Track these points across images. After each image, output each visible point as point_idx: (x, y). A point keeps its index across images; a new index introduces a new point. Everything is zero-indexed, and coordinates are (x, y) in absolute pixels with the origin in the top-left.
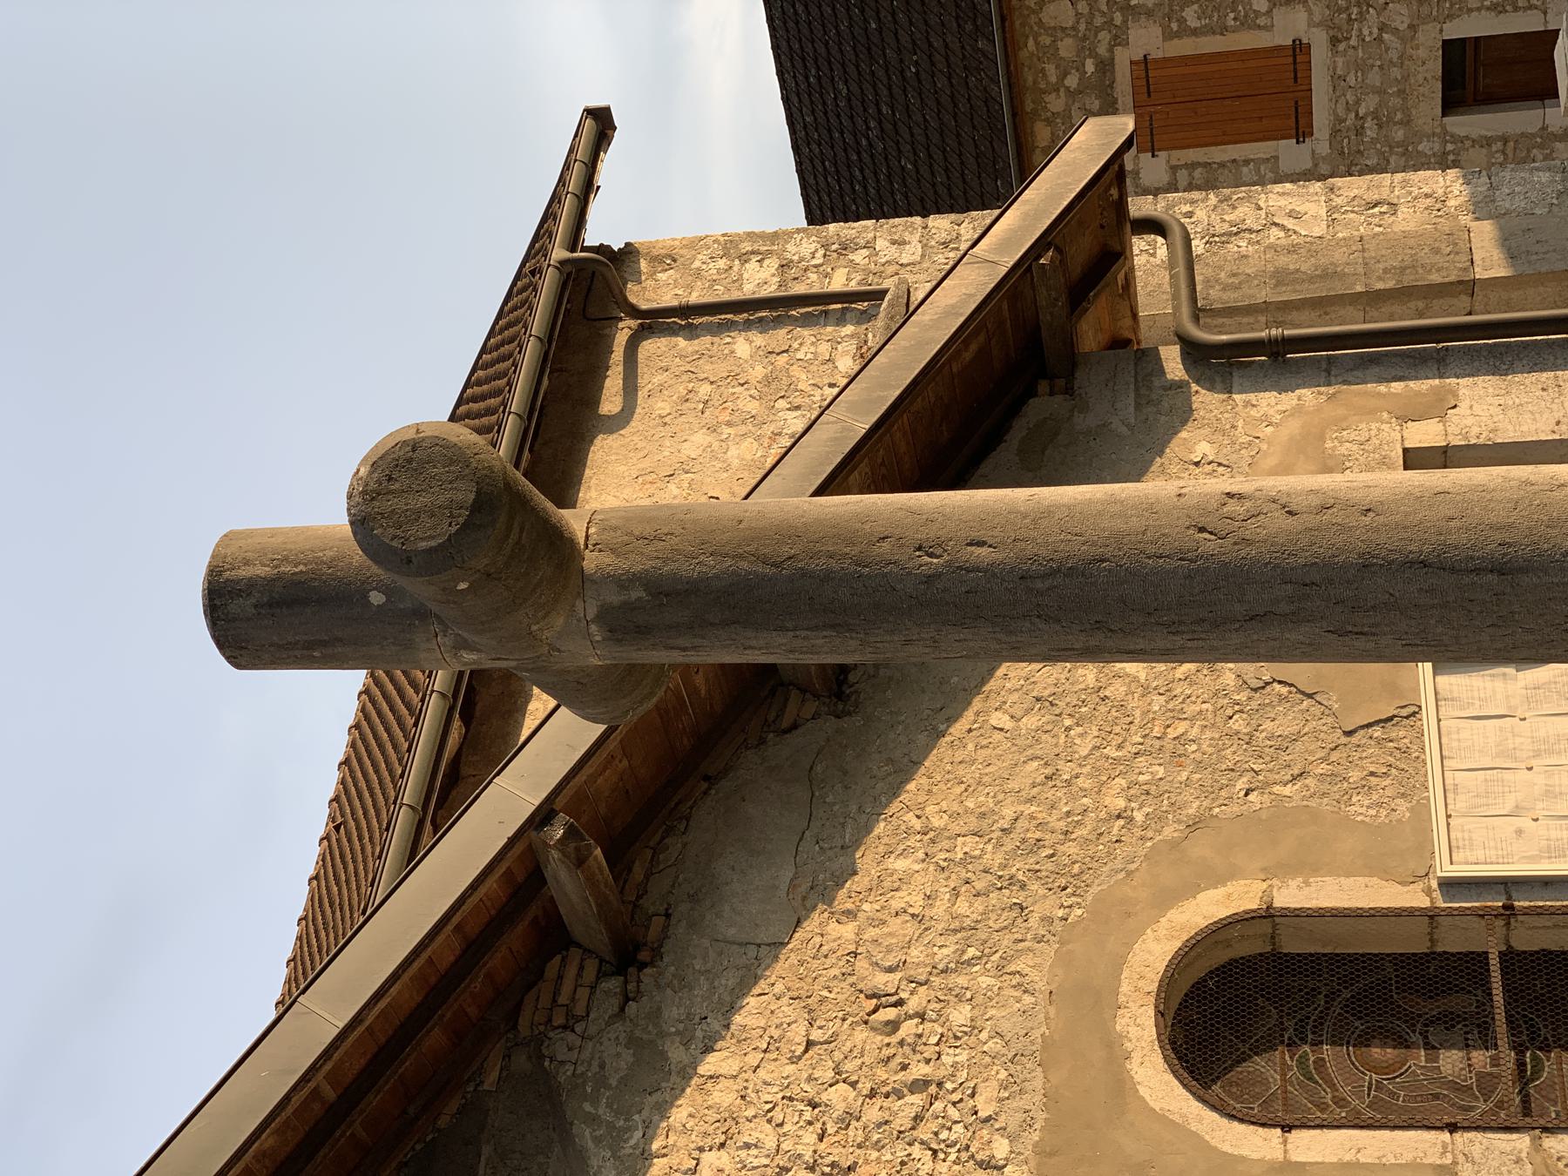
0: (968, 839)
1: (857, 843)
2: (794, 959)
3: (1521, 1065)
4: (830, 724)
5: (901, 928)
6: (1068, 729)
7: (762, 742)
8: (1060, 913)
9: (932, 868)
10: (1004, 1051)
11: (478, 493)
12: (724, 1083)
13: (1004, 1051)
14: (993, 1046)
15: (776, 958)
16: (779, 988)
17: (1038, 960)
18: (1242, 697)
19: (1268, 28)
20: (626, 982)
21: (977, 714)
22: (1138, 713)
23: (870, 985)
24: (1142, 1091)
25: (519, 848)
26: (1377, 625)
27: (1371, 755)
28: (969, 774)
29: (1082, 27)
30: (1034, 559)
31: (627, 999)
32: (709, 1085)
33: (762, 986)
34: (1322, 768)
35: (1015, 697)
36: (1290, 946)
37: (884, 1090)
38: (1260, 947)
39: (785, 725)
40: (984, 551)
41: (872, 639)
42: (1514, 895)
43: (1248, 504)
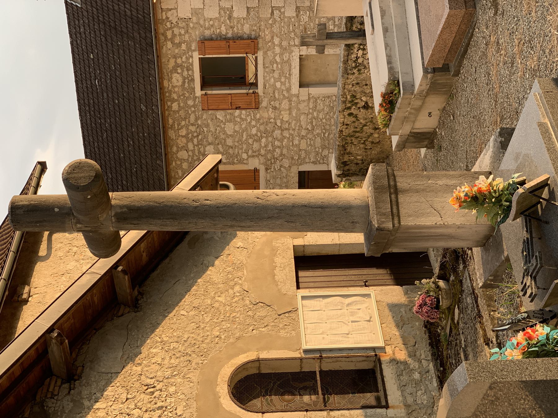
0: (174, 343)
1: (142, 345)
2: (122, 377)
3: (324, 399)
4: (133, 314)
5: (156, 367)
6: (203, 315)
7: (112, 319)
8: (201, 362)
9: (164, 351)
10: (185, 398)
11: (96, 174)
12: (101, 410)
13: (185, 398)
14: (182, 397)
15: (117, 377)
16: (118, 384)
17: (195, 374)
18: (251, 306)
19: (247, 164)
20: (70, 385)
21: (177, 311)
22: (222, 311)
23: (145, 382)
24: (224, 406)
25: (42, 340)
26: (296, 220)
27: (285, 320)
28: (174, 327)
29: (190, 159)
30: (220, 203)
31: (70, 390)
32: (97, 411)
33: (113, 384)
34: (273, 324)
35: (187, 307)
36: (264, 371)
37: (150, 410)
38: (255, 371)
39: (119, 315)
40: (208, 202)
41: (181, 222)
42: (322, 353)
43: (268, 194)
